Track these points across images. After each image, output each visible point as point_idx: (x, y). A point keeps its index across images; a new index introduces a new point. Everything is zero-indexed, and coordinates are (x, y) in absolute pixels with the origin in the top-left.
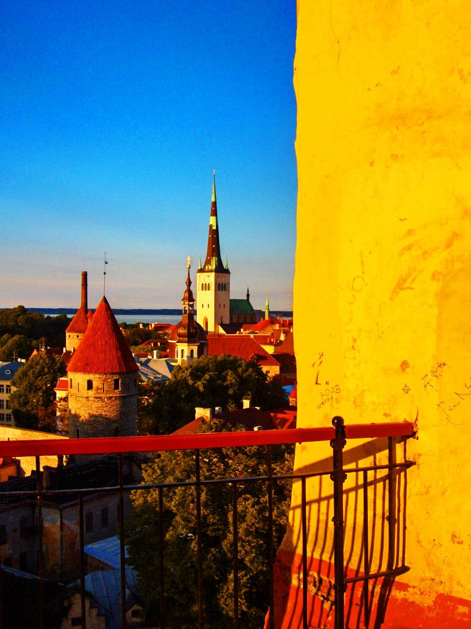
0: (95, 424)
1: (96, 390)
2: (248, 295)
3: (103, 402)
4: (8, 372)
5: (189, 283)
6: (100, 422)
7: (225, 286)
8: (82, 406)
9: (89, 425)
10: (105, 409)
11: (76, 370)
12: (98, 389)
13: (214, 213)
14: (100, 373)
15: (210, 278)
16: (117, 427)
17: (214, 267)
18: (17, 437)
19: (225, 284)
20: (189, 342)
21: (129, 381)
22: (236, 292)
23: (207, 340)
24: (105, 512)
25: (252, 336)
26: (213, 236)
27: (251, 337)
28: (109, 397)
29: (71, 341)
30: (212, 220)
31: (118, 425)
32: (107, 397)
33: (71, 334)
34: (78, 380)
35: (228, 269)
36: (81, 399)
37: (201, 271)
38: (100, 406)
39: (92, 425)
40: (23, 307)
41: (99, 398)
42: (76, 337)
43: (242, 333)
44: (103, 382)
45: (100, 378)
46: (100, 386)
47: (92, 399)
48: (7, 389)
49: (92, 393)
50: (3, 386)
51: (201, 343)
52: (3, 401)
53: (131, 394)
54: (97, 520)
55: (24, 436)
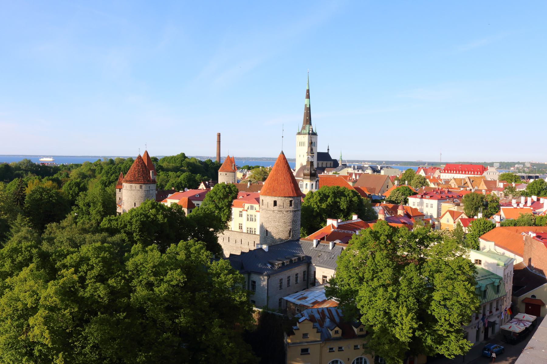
1: (279, 207)
2: (328, 149)
4: (197, 196)
8: (269, 216)
10: (284, 218)
11: (266, 194)
13: (308, 97)
15: (305, 139)
17: (308, 131)
20: (311, 179)
22: (321, 148)
24: (289, 277)
25: (337, 176)
26: (307, 112)
30: (306, 101)
33: (221, 173)
36: (269, 212)
37: (299, 134)
40: (183, 154)
46: (282, 204)
47: (277, 212)
53: (299, 209)
54: (285, 282)
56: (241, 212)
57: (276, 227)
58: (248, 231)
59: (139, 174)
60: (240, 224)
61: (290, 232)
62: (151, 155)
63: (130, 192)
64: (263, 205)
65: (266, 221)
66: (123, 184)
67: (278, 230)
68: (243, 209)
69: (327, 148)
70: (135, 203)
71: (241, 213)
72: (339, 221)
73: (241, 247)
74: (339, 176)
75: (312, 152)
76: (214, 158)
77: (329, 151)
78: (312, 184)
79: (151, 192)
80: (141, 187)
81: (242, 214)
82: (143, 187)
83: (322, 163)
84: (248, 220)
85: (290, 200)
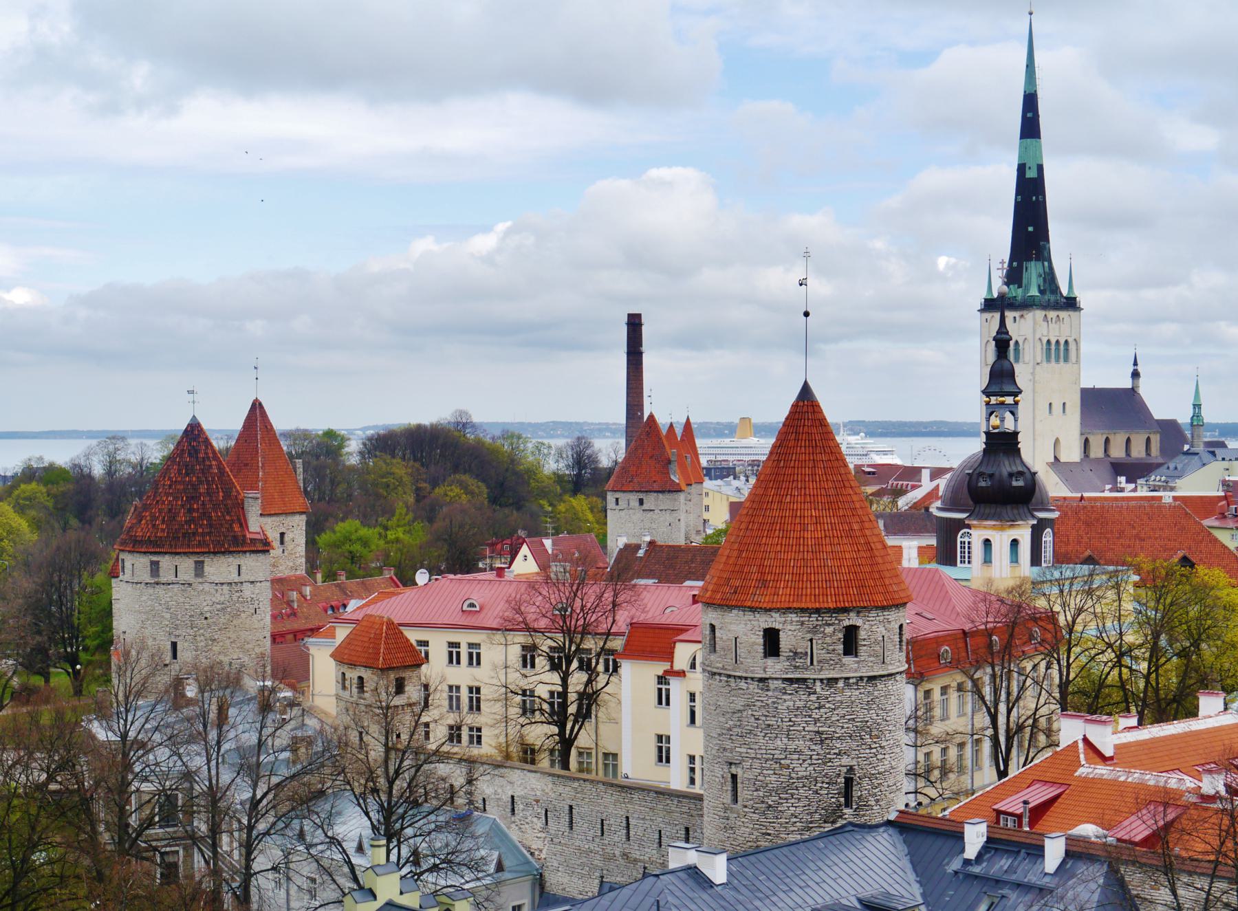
0: (786, 758)
1: (788, 658)
2: (1136, 375)
3: (809, 695)
4: (472, 605)
5: (1002, 343)
6: (800, 753)
7: (1067, 350)
9: (767, 760)
12: (796, 653)
13: (1030, 128)
14: (803, 610)
16: (851, 769)
17: (1034, 292)
18: (538, 793)
19: (1066, 342)
21: (884, 632)
23: (1053, 510)
27: (1171, 500)
28: (829, 680)
29: (622, 513)
31: (856, 763)
32: (821, 680)
33: (618, 495)
34: (733, 627)
35: (1075, 298)
36: (743, 684)
38: (799, 704)
39: (777, 761)
41: (798, 680)
42: (637, 504)
43: (1122, 490)
44: (809, 636)
45: (802, 623)
47: (779, 684)
48: (471, 655)
49: (778, 667)
50: (457, 645)
51: (1041, 520)
52: (458, 688)
55: (561, 789)
56: (662, 679)
57: (777, 761)
58: (692, 770)
59: (191, 510)
60: (660, 738)
61: (849, 782)
62: (281, 420)
63: (151, 591)
64: (713, 647)
65: (730, 729)
66: (122, 556)
67: (785, 772)
68: (667, 666)
69: (1131, 369)
70: (174, 645)
71: (664, 687)
72: (1125, 722)
73: (625, 855)
74: (1175, 498)
75: (1012, 389)
76: (604, 429)
77: (1142, 381)
78: (1015, 543)
79: (248, 590)
80: (199, 568)
81: (668, 691)
82: (207, 568)
83: (1107, 441)
84: (693, 721)
85: (846, 623)
